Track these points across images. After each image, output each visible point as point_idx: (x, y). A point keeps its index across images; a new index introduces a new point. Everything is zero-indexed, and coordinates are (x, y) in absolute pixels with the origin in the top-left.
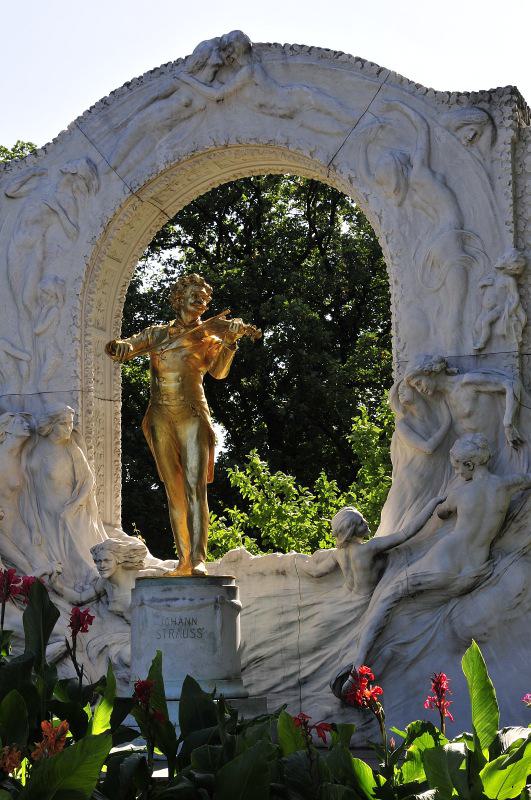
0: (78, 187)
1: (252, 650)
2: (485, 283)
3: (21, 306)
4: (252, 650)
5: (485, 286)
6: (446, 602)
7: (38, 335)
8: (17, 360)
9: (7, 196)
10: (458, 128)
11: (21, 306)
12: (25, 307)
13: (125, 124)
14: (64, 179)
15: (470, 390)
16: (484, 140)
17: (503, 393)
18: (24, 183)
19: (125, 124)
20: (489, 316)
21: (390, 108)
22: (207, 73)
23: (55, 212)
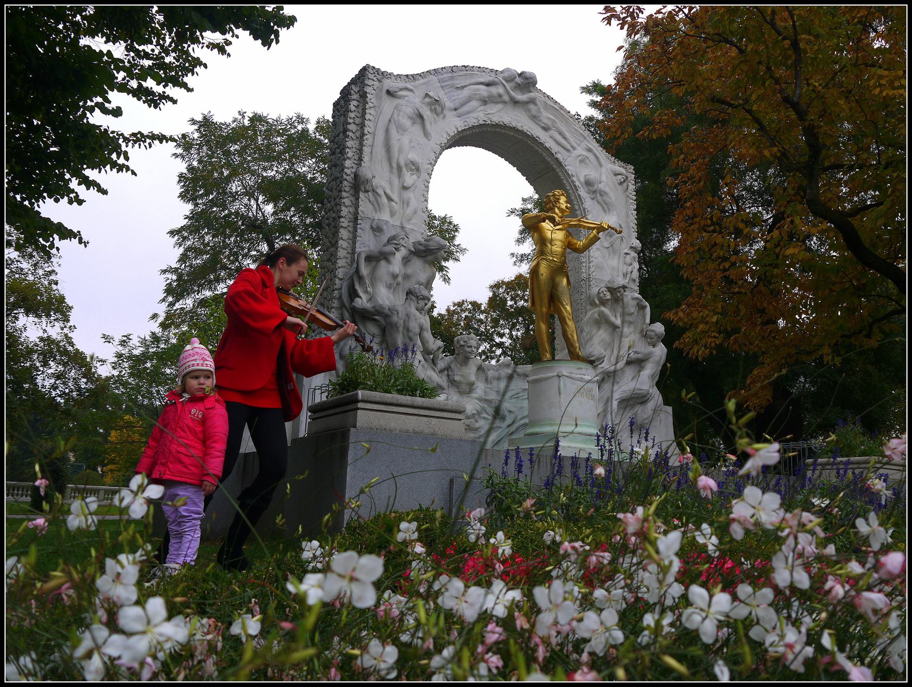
0: (435, 109)
1: (521, 419)
2: (626, 251)
3: (395, 165)
4: (521, 419)
5: (627, 254)
6: (633, 406)
7: (405, 188)
8: (390, 199)
9: (388, 92)
10: (616, 175)
11: (395, 165)
12: (399, 168)
13: (463, 87)
14: (427, 100)
15: (635, 303)
16: (625, 184)
17: (644, 308)
18: (401, 89)
19: (463, 87)
20: (630, 269)
21: (590, 150)
22: (512, 84)
23: (421, 117)
